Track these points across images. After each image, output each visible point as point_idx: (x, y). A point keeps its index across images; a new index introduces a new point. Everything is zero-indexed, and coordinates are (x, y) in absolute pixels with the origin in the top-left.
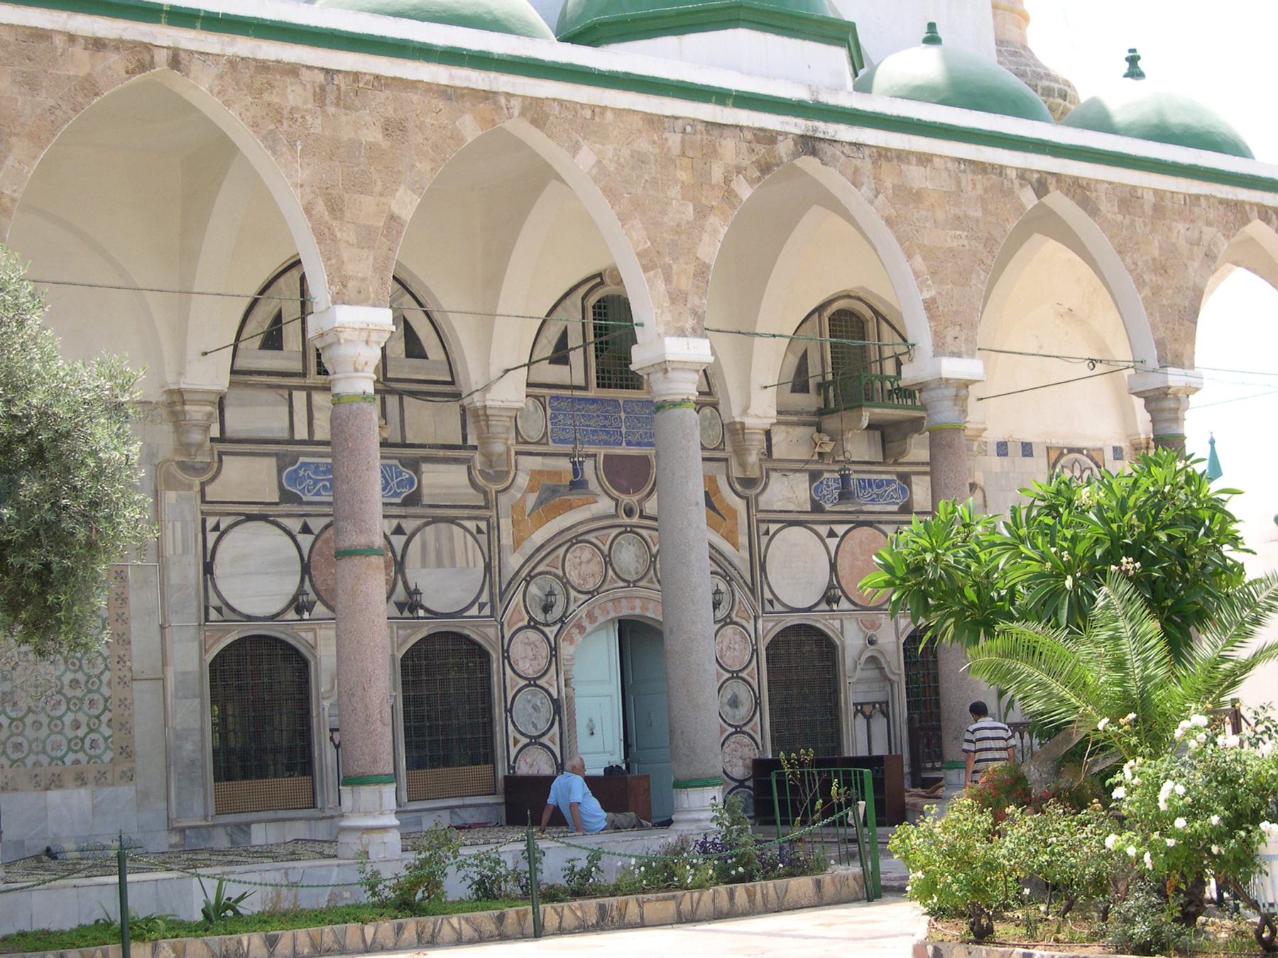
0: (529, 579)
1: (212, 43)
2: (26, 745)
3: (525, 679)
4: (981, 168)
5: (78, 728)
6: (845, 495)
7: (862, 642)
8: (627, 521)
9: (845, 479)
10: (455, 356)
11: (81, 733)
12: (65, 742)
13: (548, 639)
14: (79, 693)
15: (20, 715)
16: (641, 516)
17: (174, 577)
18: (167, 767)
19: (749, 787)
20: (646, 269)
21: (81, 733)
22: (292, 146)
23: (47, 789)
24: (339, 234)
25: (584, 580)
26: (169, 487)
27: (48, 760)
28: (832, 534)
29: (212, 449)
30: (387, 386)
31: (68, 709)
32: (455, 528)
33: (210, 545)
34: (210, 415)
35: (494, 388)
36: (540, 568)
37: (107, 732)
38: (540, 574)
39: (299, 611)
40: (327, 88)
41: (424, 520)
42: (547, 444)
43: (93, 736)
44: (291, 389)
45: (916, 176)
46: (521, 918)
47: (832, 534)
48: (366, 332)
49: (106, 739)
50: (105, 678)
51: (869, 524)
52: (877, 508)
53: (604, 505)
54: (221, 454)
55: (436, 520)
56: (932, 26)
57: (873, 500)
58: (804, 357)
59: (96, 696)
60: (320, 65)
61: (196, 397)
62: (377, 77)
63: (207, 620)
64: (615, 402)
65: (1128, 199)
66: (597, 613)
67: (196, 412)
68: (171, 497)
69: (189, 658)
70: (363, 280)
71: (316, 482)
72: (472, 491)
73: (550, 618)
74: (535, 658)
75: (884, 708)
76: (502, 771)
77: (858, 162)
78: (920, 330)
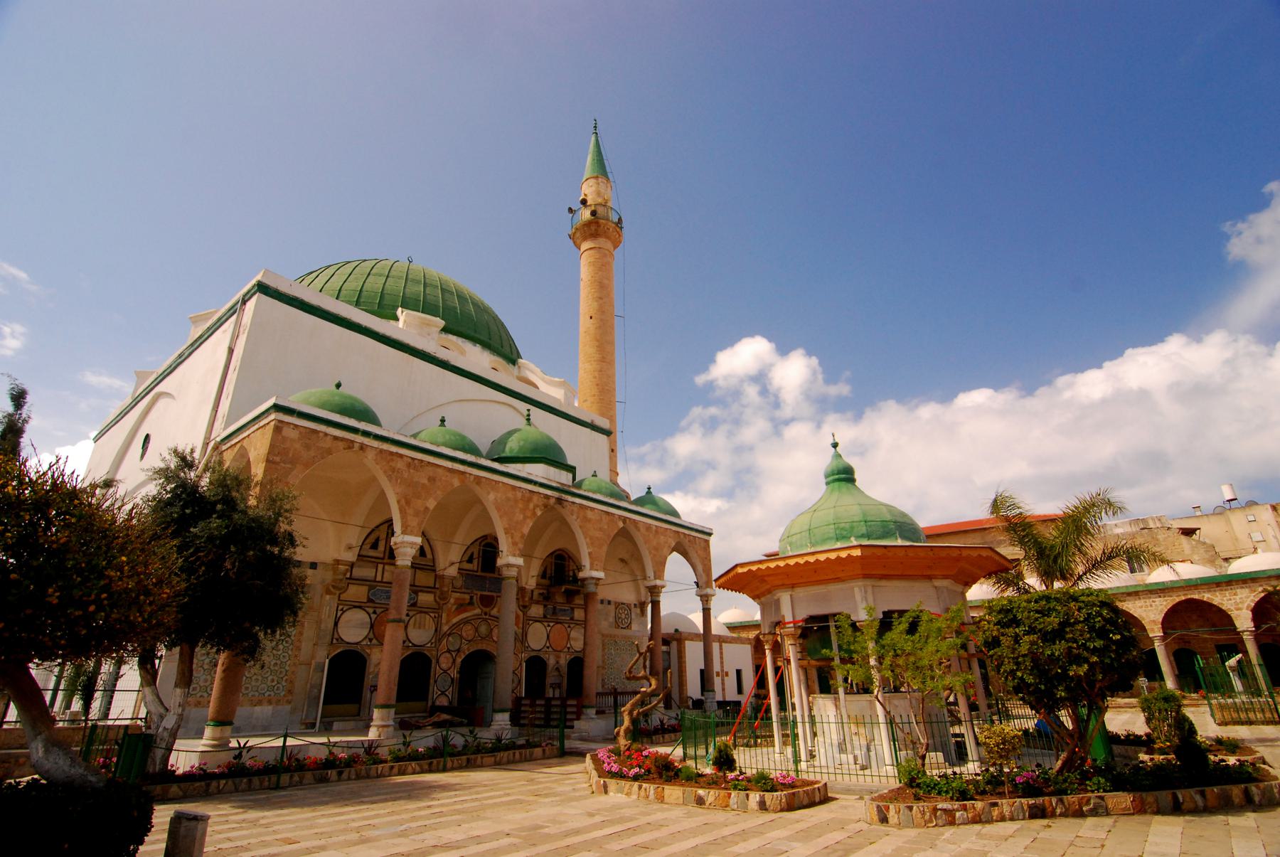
1: (375, 444)
4: (608, 513)
6: (554, 613)
9: (554, 608)
17: (323, 626)
30: (414, 566)
45: (589, 514)
46: (438, 763)
48: (413, 544)
53: (478, 611)
65: (648, 527)
68: (328, 597)
69: (323, 657)
75: (559, 686)
76: (430, 703)
78: (586, 562)
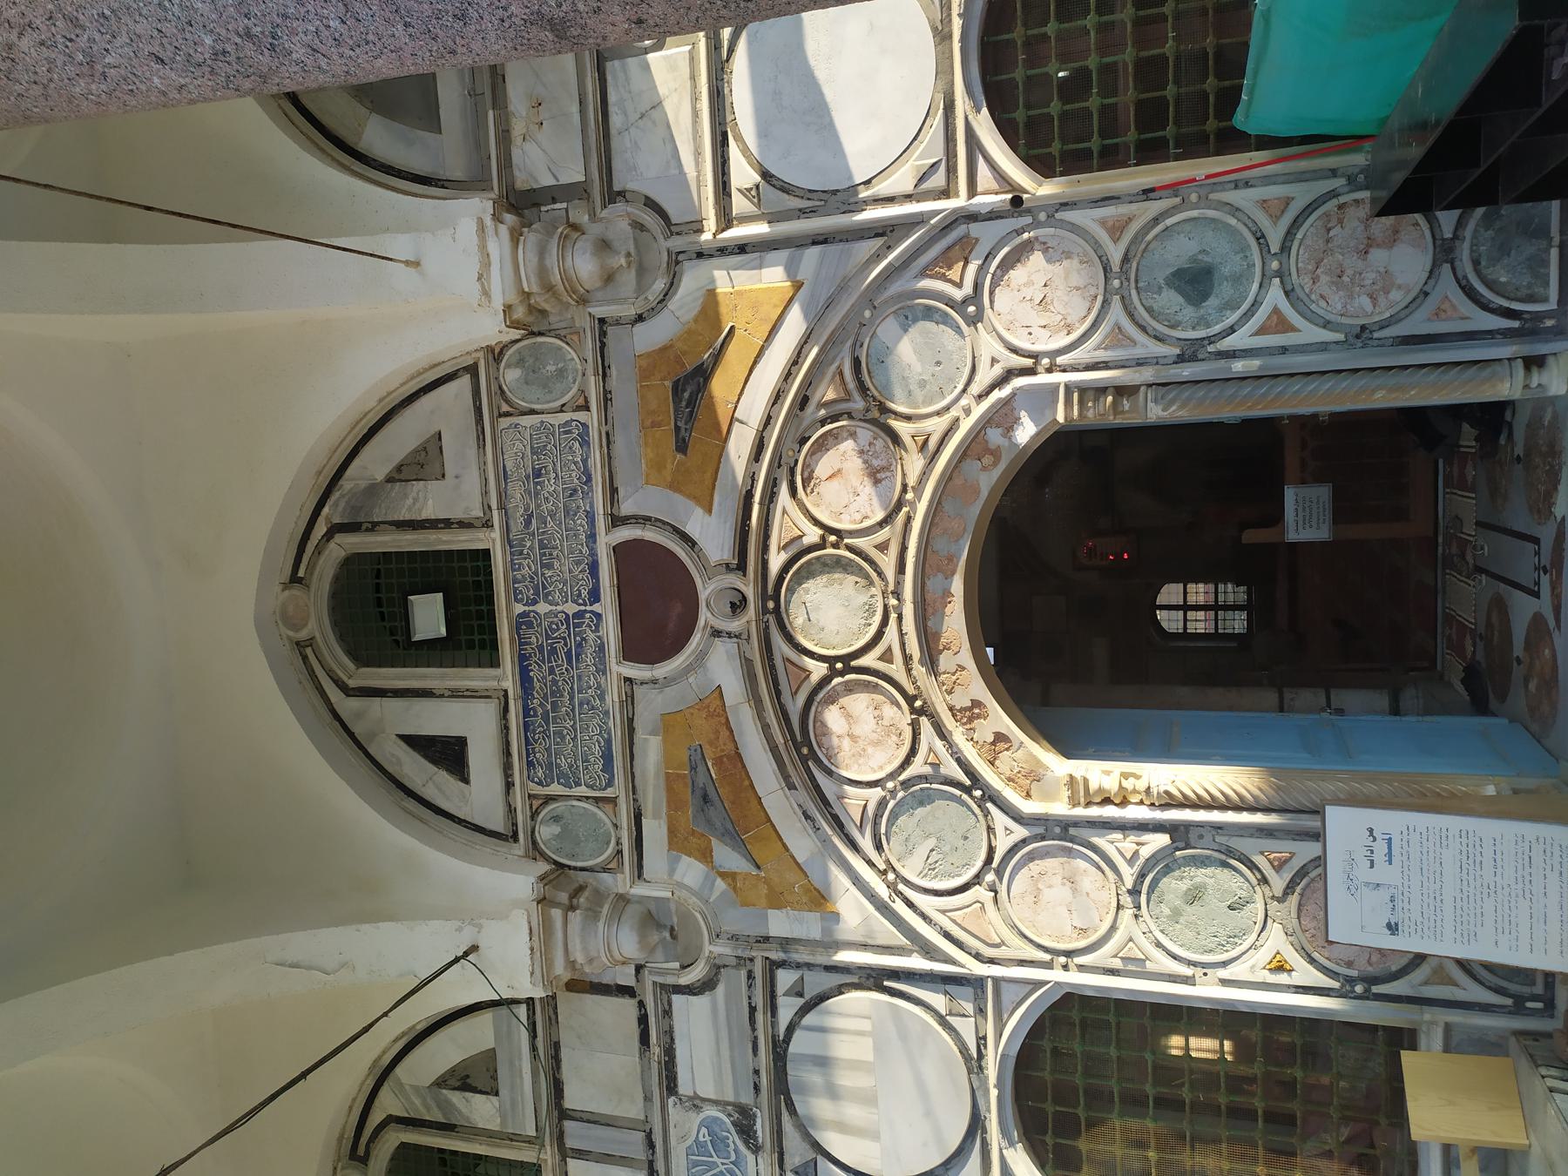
8: (751, 611)
16: (742, 567)
19: (1460, 224)
32: (792, 1049)
41: (785, 1117)
53: (723, 670)
64: (522, 623)
72: (720, 989)
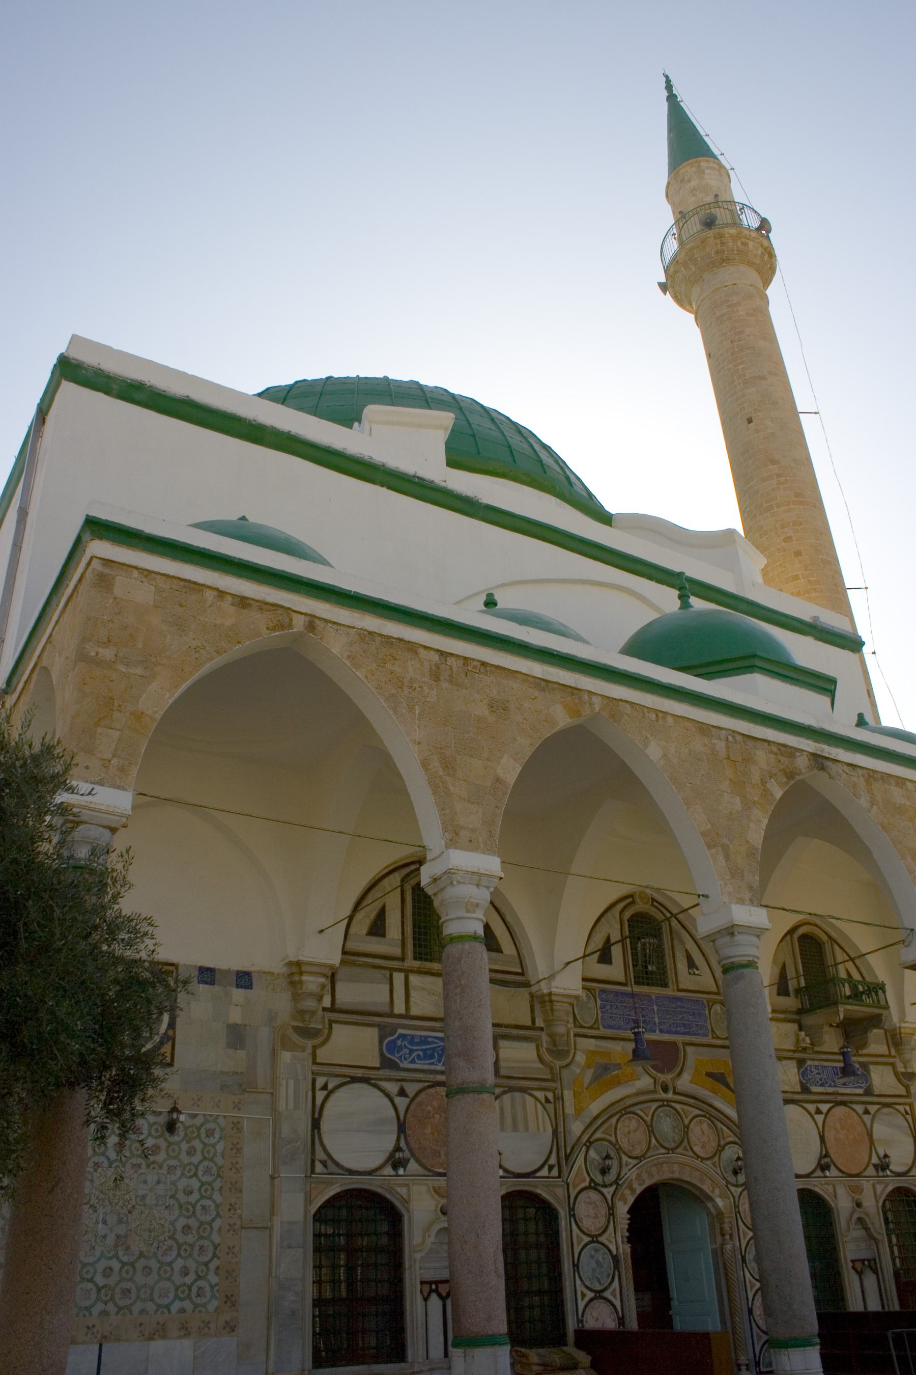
0: (589, 1144)
2: (134, 1290)
3: (588, 1235)
5: (187, 1274)
7: (851, 1205)
8: (664, 1096)
10: (524, 952)
11: (188, 1280)
12: (172, 1289)
13: (605, 1198)
14: (190, 1239)
15: (132, 1259)
16: (675, 1093)
18: (269, 1319)
20: (710, 847)
21: (188, 1280)
22: (411, 709)
23: (151, 1338)
24: (452, 789)
25: (633, 1146)
26: (284, 1047)
27: (155, 1307)
28: (818, 1112)
29: (323, 1017)
31: (179, 1255)
32: (527, 1097)
33: (319, 1102)
34: (323, 987)
35: (558, 977)
36: (598, 1135)
37: (214, 1279)
38: (597, 1140)
39: (395, 1167)
40: (442, 667)
42: (598, 1029)
43: (201, 1283)
44: (392, 970)
47: (818, 1112)
48: (478, 878)
49: (212, 1287)
50: (217, 1224)
51: (844, 1103)
52: (848, 1091)
53: (645, 1082)
54: (331, 1022)
55: (511, 1089)
56: (860, 716)
57: (844, 1084)
58: (784, 968)
59: (206, 1243)
60: (437, 647)
61: (313, 969)
62: (484, 664)
63: (313, 1172)
64: (648, 997)
66: (645, 1176)
67: (312, 983)
68: (286, 1056)
69: (295, 1209)
70: (473, 830)
71: (412, 1051)
72: (540, 1065)
73: (607, 1181)
74: (596, 1217)
77: (855, 779)
